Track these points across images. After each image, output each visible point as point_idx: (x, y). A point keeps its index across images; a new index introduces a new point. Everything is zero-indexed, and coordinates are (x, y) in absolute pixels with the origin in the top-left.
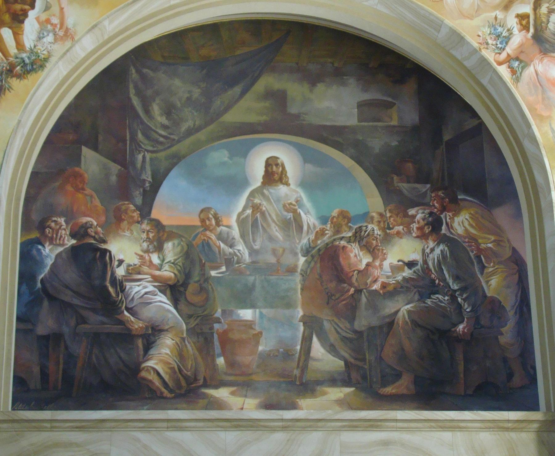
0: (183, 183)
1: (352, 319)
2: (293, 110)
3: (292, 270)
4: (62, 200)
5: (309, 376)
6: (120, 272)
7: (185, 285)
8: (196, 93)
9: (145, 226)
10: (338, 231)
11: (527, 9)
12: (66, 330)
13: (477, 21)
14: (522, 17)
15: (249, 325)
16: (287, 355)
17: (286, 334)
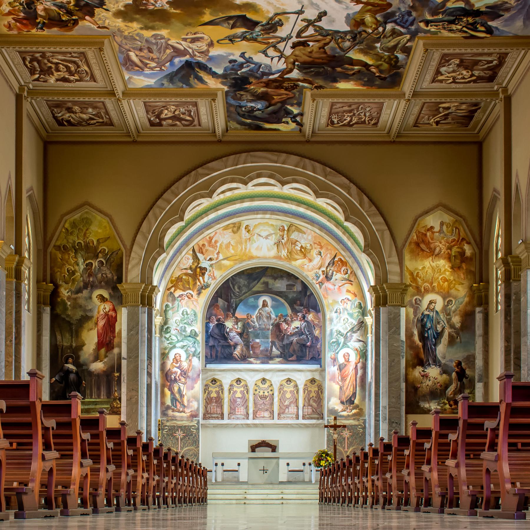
0: (242, 307)
1: (282, 341)
2: (270, 287)
3: (268, 329)
4: (214, 312)
5: (272, 355)
6: (228, 330)
7: (243, 333)
8: (246, 282)
9: (234, 318)
10: (280, 319)
11: (324, 269)
12: (216, 344)
13: (312, 273)
14: (323, 271)
15: (258, 343)
16: (267, 350)
17: (267, 345)
